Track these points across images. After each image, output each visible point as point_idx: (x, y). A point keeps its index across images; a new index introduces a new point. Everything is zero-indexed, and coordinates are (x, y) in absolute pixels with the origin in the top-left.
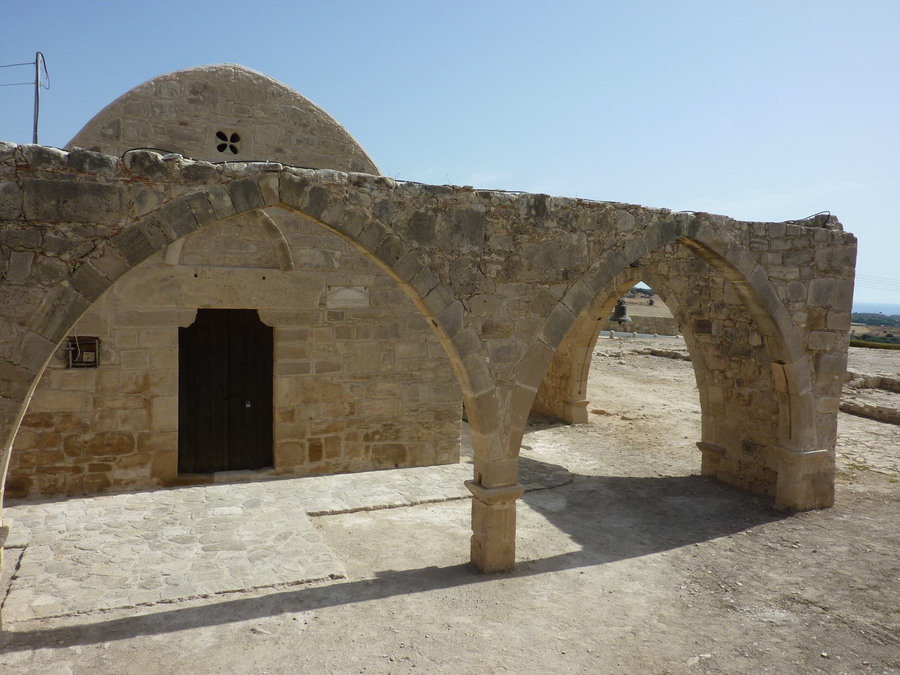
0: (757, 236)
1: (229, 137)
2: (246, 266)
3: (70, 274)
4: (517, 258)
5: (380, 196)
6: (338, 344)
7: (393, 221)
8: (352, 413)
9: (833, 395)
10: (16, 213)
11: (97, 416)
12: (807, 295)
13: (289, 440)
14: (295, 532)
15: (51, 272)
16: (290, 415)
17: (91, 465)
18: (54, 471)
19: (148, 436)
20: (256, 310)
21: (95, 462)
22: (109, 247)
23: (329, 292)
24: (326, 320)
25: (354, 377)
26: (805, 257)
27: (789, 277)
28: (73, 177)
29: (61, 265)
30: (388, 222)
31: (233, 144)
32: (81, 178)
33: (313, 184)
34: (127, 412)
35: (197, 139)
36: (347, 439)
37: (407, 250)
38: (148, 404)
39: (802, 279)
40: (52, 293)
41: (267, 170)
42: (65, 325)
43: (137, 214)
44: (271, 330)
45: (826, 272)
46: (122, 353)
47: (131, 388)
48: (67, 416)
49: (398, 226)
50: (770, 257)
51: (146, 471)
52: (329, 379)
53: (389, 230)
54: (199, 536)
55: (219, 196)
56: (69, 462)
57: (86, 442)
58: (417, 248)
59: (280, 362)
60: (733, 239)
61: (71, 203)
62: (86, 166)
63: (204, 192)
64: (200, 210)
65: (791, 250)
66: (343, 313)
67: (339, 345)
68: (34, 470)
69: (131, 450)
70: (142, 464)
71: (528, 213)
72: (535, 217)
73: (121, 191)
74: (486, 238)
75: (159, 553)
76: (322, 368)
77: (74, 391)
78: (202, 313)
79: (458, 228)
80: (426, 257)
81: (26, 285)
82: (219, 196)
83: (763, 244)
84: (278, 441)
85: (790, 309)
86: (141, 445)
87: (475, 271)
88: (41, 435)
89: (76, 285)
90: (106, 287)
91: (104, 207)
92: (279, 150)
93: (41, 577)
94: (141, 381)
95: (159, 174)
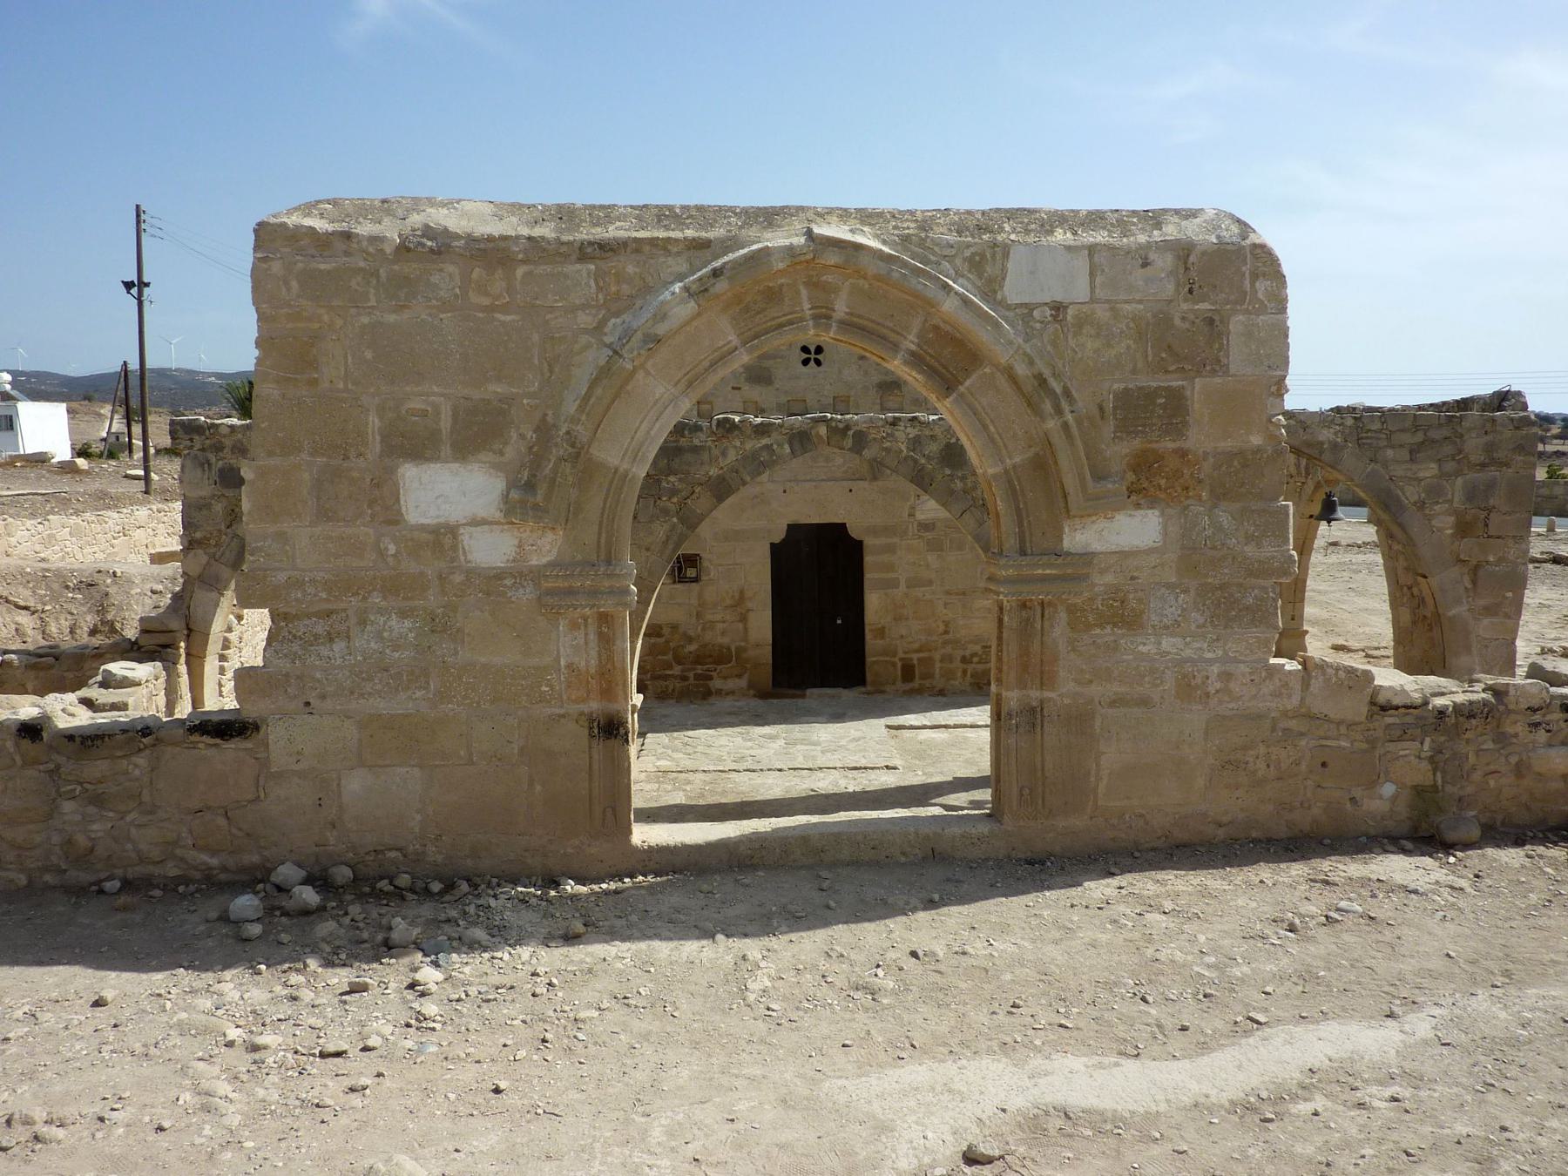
0: (1370, 430)
1: (813, 350)
2: (836, 480)
3: (677, 513)
5: (913, 432)
6: (929, 558)
9: (1507, 616)
11: (699, 628)
12: (1453, 494)
13: (882, 659)
15: (665, 512)
16: (881, 632)
17: (695, 674)
18: (666, 678)
19: (744, 650)
20: (844, 525)
21: (700, 672)
25: (948, 593)
26: (1448, 449)
27: (1421, 475)
29: (672, 508)
31: (817, 356)
32: (683, 442)
34: (725, 625)
35: (782, 357)
38: (743, 619)
39: (1443, 475)
40: (666, 527)
41: (817, 421)
42: (675, 550)
43: (721, 465)
44: (861, 543)
45: (1483, 465)
46: (720, 568)
47: (728, 602)
48: (674, 627)
50: (1390, 453)
51: (743, 683)
53: (923, 461)
55: (780, 445)
56: (677, 670)
57: (691, 653)
59: (870, 576)
60: (1332, 437)
61: (677, 460)
62: (686, 432)
64: (767, 458)
65: (1423, 443)
66: (934, 524)
67: (931, 558)
68: (649, 675)
70: (739, 676)
73: (710, 448)
75: (750, 744)
76: (913, 583)
78: (793, 529)
82: (780, 445)
83: (1379, 439)
84: (869, 659)
85: (1427, 512)
89: (682, 520)
90: (702, 520)
93: (660, 751)
94: (737, 595)
95: (736, 433)
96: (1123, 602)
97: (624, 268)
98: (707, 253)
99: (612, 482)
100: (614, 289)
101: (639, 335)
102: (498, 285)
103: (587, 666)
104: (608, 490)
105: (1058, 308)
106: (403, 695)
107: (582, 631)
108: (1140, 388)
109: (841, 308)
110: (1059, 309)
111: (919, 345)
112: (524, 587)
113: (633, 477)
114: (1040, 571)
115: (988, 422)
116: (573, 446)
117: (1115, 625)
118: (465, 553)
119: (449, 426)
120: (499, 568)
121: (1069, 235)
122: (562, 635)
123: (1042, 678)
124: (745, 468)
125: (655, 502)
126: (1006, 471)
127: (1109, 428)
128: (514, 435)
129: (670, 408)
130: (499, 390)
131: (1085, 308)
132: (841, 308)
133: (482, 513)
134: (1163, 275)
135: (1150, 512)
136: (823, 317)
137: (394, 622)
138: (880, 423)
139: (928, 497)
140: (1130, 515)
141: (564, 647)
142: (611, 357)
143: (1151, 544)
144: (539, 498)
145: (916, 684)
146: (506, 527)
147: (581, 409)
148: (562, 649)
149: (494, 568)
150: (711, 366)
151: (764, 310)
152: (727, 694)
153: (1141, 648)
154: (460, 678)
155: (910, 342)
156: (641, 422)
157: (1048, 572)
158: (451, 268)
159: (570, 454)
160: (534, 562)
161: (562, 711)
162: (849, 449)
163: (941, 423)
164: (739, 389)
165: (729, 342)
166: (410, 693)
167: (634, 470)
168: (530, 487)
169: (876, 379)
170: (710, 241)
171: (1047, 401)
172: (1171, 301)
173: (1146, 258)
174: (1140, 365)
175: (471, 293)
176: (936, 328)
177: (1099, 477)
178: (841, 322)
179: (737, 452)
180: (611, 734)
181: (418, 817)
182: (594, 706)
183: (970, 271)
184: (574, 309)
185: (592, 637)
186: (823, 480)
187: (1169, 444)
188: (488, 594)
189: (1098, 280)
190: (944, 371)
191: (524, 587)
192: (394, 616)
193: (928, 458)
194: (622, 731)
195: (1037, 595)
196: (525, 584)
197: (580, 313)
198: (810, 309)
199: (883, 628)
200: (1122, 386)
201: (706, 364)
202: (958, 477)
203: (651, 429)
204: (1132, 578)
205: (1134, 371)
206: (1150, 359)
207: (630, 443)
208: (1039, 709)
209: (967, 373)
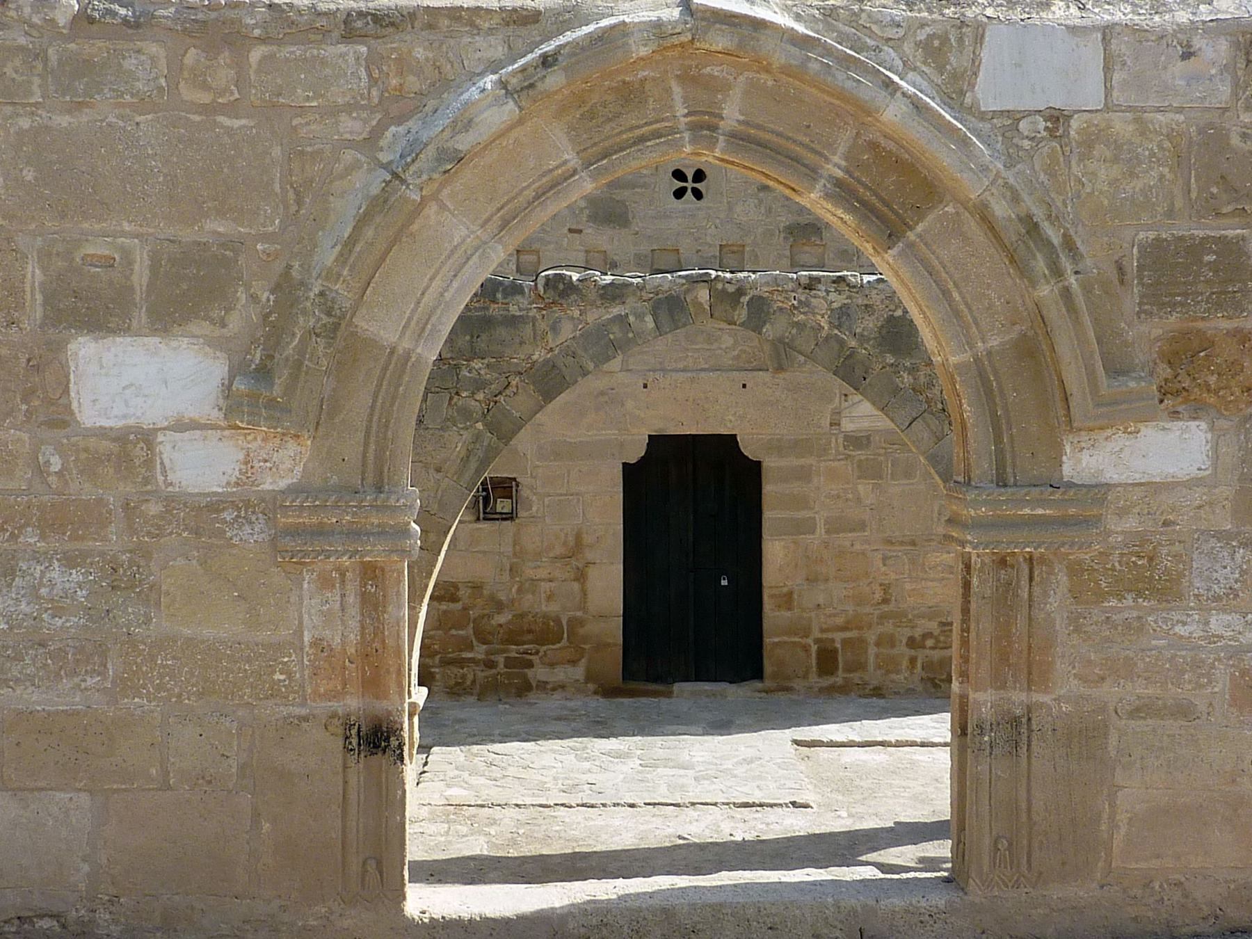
5: (838, 300)
6: (861, 488)
8: (885, 601)
14: (767, 758)
15: (466, 414)
16: (787, 600)
17: (507, 658)
18: (461, 663)
19: (582, 622)
21: (514, 655)
22: (523, 384)
23: (845, 404)
24: (841, 449)
25: (889, 542)
28: (487, 309)
30: (850, 332)
32: (494, 310)
33: (752, 293)
34: (553, 584)
35: (644, 186)
36: (878, 644)
38: (581, 576)
40: (467, 435)
41: (694, 281)
42: (479, 471)
43: (551, 345)
47: (559, 550)
48: (477, 587)
51: (579, 672)
52: (848, 544)
53: (853, 343)
54: (639, 752)
55: (639, 317)
56: (480, 652)
57: (501, 625)
58: (892, 364)
59: (771, 515)
61: (484, 337)
62: (499, 296)
63: (623, 314)
64: (619, 335)
66: (868, 438)
67: (864, 488)
68: (437, 658)
69: (560, 639)
70: (573, 662)
75: (587, 765)
77: (485, 552)
78: (657, 442)
80: (905, 375)
81: (442, 429)
82: (639, 317)
86: (571, 633)
88: (445, 612)
89: (491, 427)
90: (520, 429)
91: (517, 340)
94: (572, 543)
95: (574, 297)
96: (1151, 559)
97: (410, 52)
98: (534, 31)
99: (385, 369)
100: (394, 82)
101: (431, 151)
102: (224, 75)
103: (343, 643)
104: (381, 379)
105: (1057, 118)
106: (66, 684)
107: (337, 591)
108: (1181, 238)
109: (732, 114)
110: (1058, 119)
111: (847, 172)
112: (251, 523)
113: (418, 361)
114: (1027, 511)
115: (951, 285)
116: (329, 314)
117: (1140, 594)
118: (164, 472)
119: (145, 281)
120: (215, 494)
121: (1074, 10)
122: (306, 594)
123: (1030, 673)
124: (586, 350)
125: (451, 399)
126: (977, 360)
127: (1131, 299)
128: (242, 296)
129: (475, 259)
130: (221, 229)
131: (1097, 118)
132: (732, 114)
133: (192, 413)
134: (1213, 71)
135: (1193, 424)
136: (704, 128)
137: (55, 574)
138: (790, 286)
139: (860, 397)
140: (1164, 429)
141: (310, 615)
142: (388, 183)
143: (1194, 472)
144: (277, 390)
145: (839, 678)
146: (227, 433)
147: (342, 259)
148: (306, 616)
149: (208, 495)
150: (537, 197)
151: (618, 115)
152: (554, 689)
153: (1179, 629)
154: (153, 659)
155: (835, 166)
156: (432, 279)
157: (1040, 511)
158: (153, 48)
159: (325, 325)
160: (267, 487)
161: (304, 712)
162: (742, 325)
163: (881, 286)
164: (580, 231)
165: (565, 162)
166: (76, 680)
167: (419, 350)
168: (264, 373)
169: (784, 220)
170: (539, 13)
171: (1038, 255)
172: (1225, 110)
173: (1190, 46)
174: (1179, 203)
175: (182, 85)
176: (873, 146)
177: (1117, 370)
178: (733, 135)
179: (576, 327)
180: (377, 747)
181: (86, 868)
182: (353, 703)
183: (924, 63)
184: (333, 111)
185: (351, 599)
186: (702, 370)
187: (1222, 324)
188: (197, 533)
189: (1117, 77)
190: (885, 209)
191: (251, 523)
192: (56, 564)
194: (394, 742)
195: (1022, 546)
196: (254, 519)
197: (343, 117)
198: (685, 116)
199: (791, 593)
200: (1152, 235)
201: (530, 193)
203: (446, 290)
204: (1166, 523)
205: (1170, 213)
206: (1194, 195)
207: (414, 311)
208: (1024, 720)
209: (920, 213)
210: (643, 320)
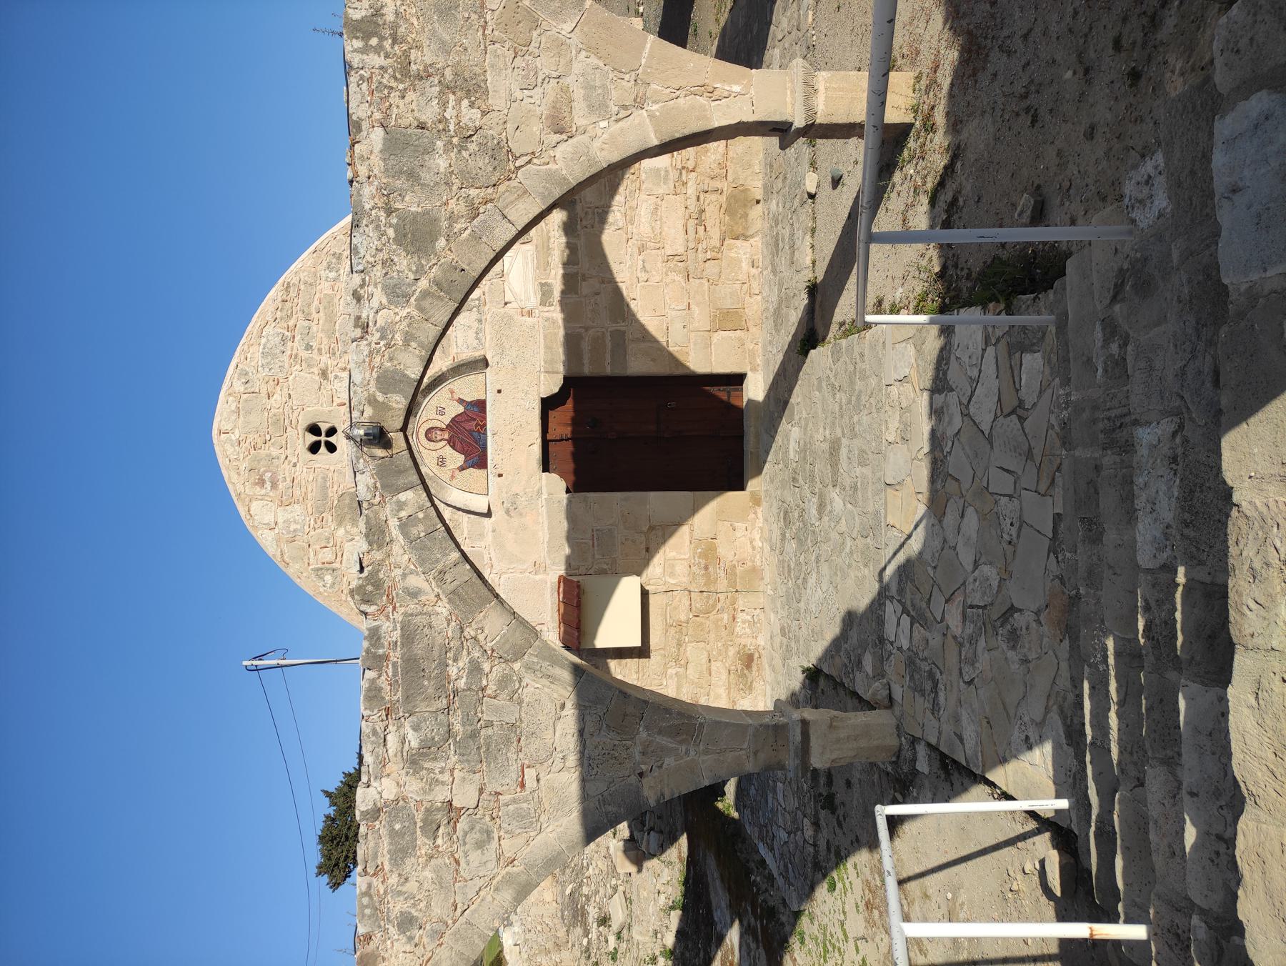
3: (506, 661)
4: (448, 72)
5: (379, 297)
7: (412, 276)
10: (441, 717)
14: (828, 372)
15: (504, 682)
22: (473, 624)
30: (413, 285)
32: (395, 656)
33: (372, 388)
35: (325, 479)
37: (451, 256)
46: (597, 557)
49: (417, 269)
55: (401, 506)
58: (447, 240)
61: (425, 665)
62: (381, 651)
63: (398, 523)
64: (421, 527)
66: (542, 285)
71: (378, 49)
72: (382, 39)
74: (422, 126)
79: (412, 176)
81: (520, 703)
82: (401, 506)
87: (472, 147)
89: (518, 654)
91: (426, 631)
92: (324, 374)
124: (437, 561)
193: (420, 272)
202: (451, 226)
210: (405, 503)
